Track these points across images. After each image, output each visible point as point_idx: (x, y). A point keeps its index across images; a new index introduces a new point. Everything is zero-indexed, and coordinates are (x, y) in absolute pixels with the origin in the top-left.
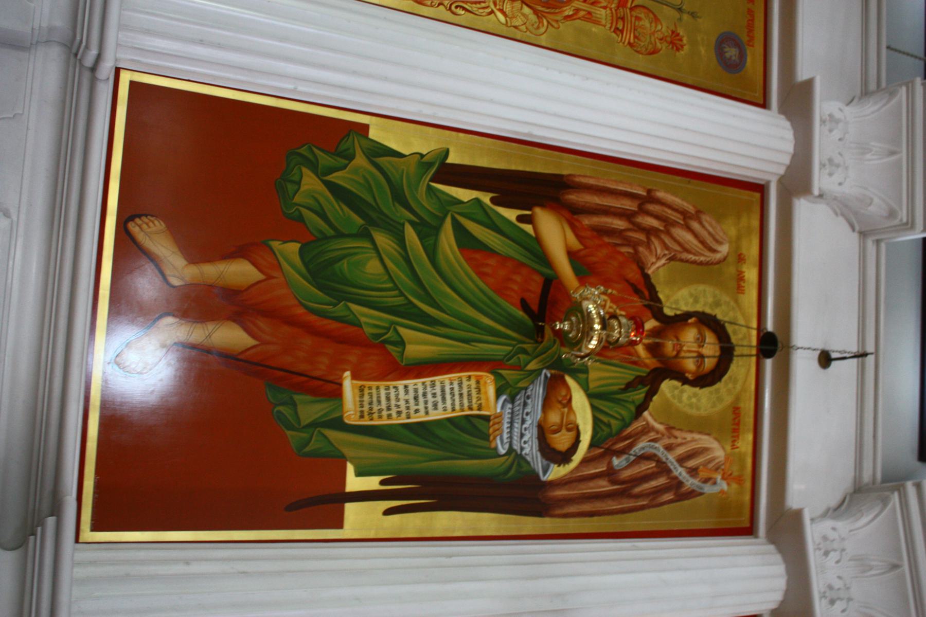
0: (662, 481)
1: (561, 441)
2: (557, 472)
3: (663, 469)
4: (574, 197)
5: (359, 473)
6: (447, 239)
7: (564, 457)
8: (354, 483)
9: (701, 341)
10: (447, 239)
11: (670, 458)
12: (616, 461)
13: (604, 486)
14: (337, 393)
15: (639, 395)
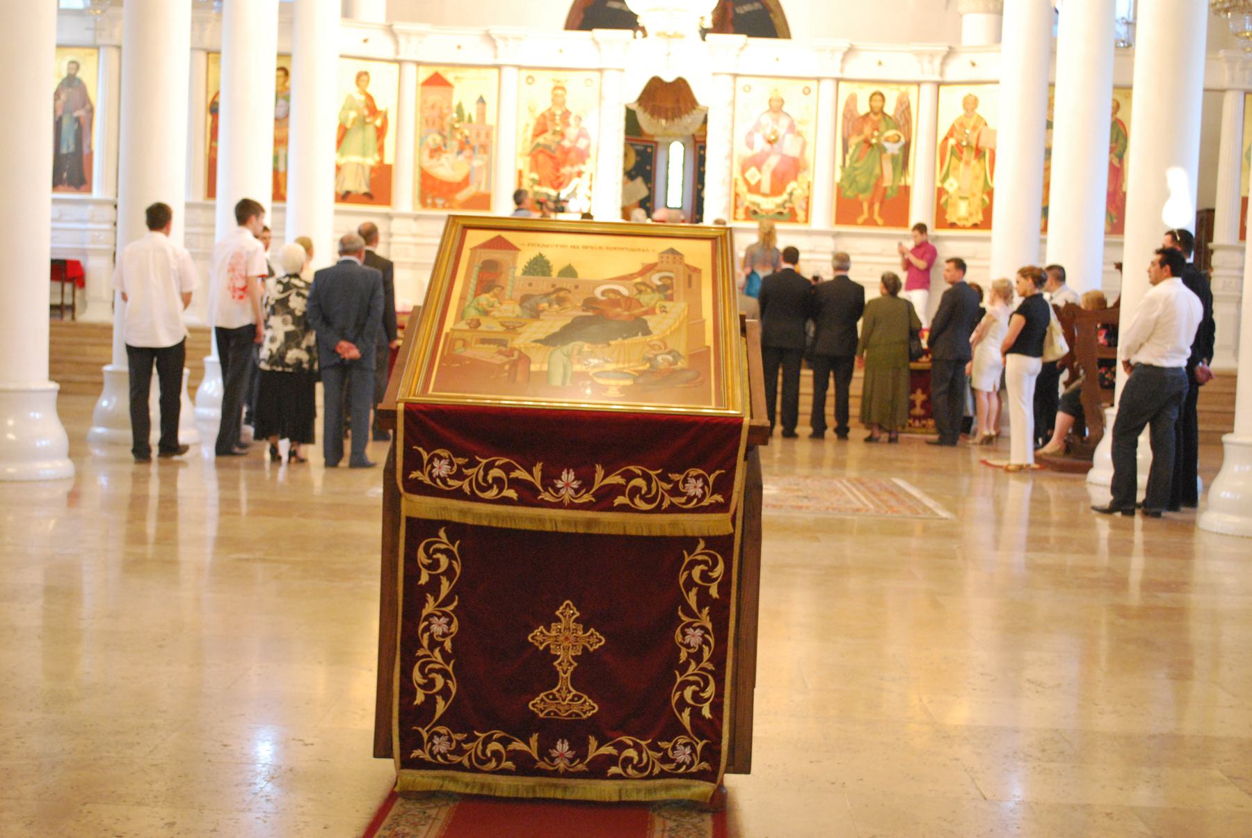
0: (906, 112)
1: (896, 138)
2: (903, 140)
3: (903, 112)
4: (846, 135)
5: (900, 181)
6: (857, 165)
7: (900, 137)
8: (902, 183)
9: (876, 101)
10: (857, 165)
11: (901, 109)
12: (901, 123)
13: (906, 127)
14: (885, 189)
15: (887, 118)
